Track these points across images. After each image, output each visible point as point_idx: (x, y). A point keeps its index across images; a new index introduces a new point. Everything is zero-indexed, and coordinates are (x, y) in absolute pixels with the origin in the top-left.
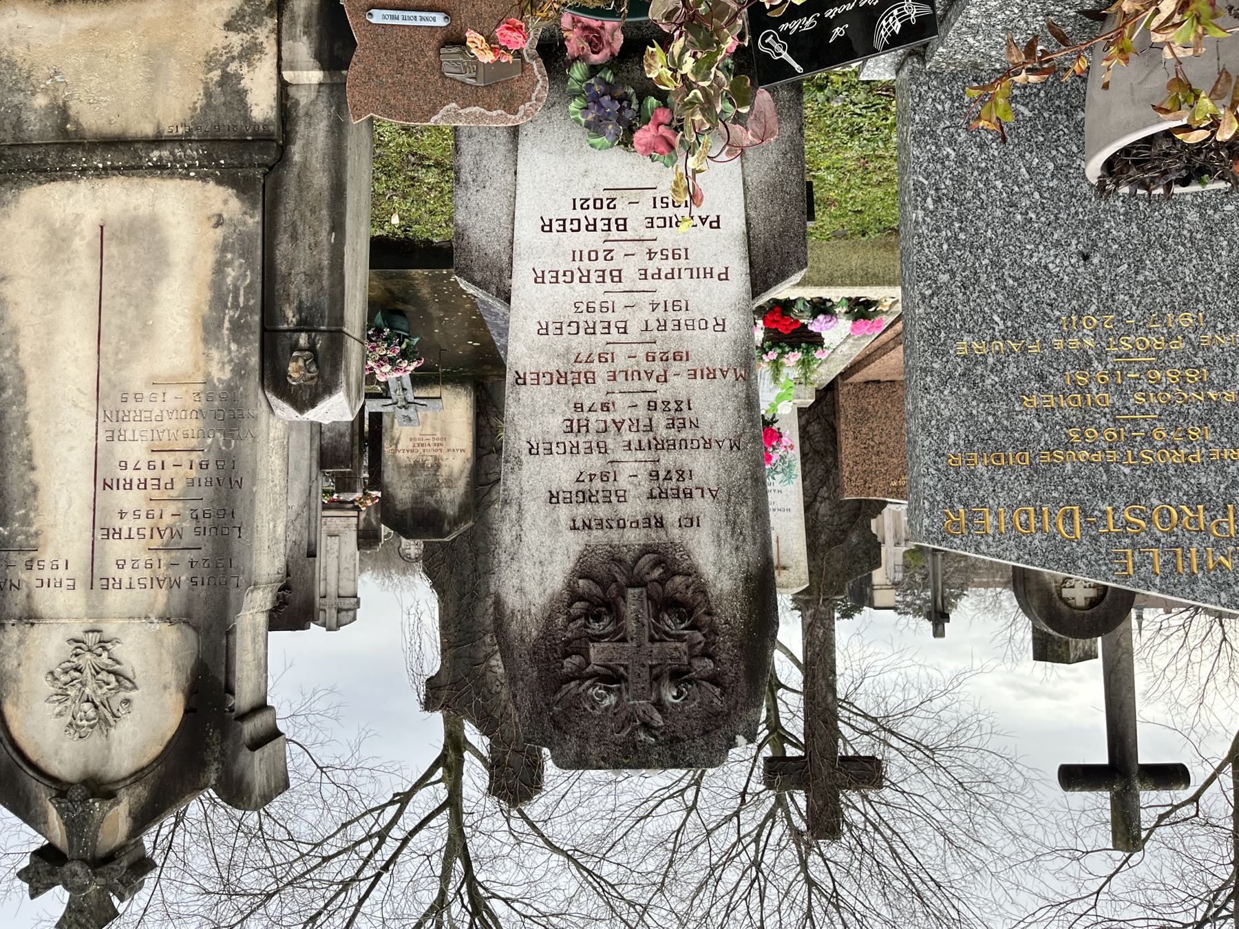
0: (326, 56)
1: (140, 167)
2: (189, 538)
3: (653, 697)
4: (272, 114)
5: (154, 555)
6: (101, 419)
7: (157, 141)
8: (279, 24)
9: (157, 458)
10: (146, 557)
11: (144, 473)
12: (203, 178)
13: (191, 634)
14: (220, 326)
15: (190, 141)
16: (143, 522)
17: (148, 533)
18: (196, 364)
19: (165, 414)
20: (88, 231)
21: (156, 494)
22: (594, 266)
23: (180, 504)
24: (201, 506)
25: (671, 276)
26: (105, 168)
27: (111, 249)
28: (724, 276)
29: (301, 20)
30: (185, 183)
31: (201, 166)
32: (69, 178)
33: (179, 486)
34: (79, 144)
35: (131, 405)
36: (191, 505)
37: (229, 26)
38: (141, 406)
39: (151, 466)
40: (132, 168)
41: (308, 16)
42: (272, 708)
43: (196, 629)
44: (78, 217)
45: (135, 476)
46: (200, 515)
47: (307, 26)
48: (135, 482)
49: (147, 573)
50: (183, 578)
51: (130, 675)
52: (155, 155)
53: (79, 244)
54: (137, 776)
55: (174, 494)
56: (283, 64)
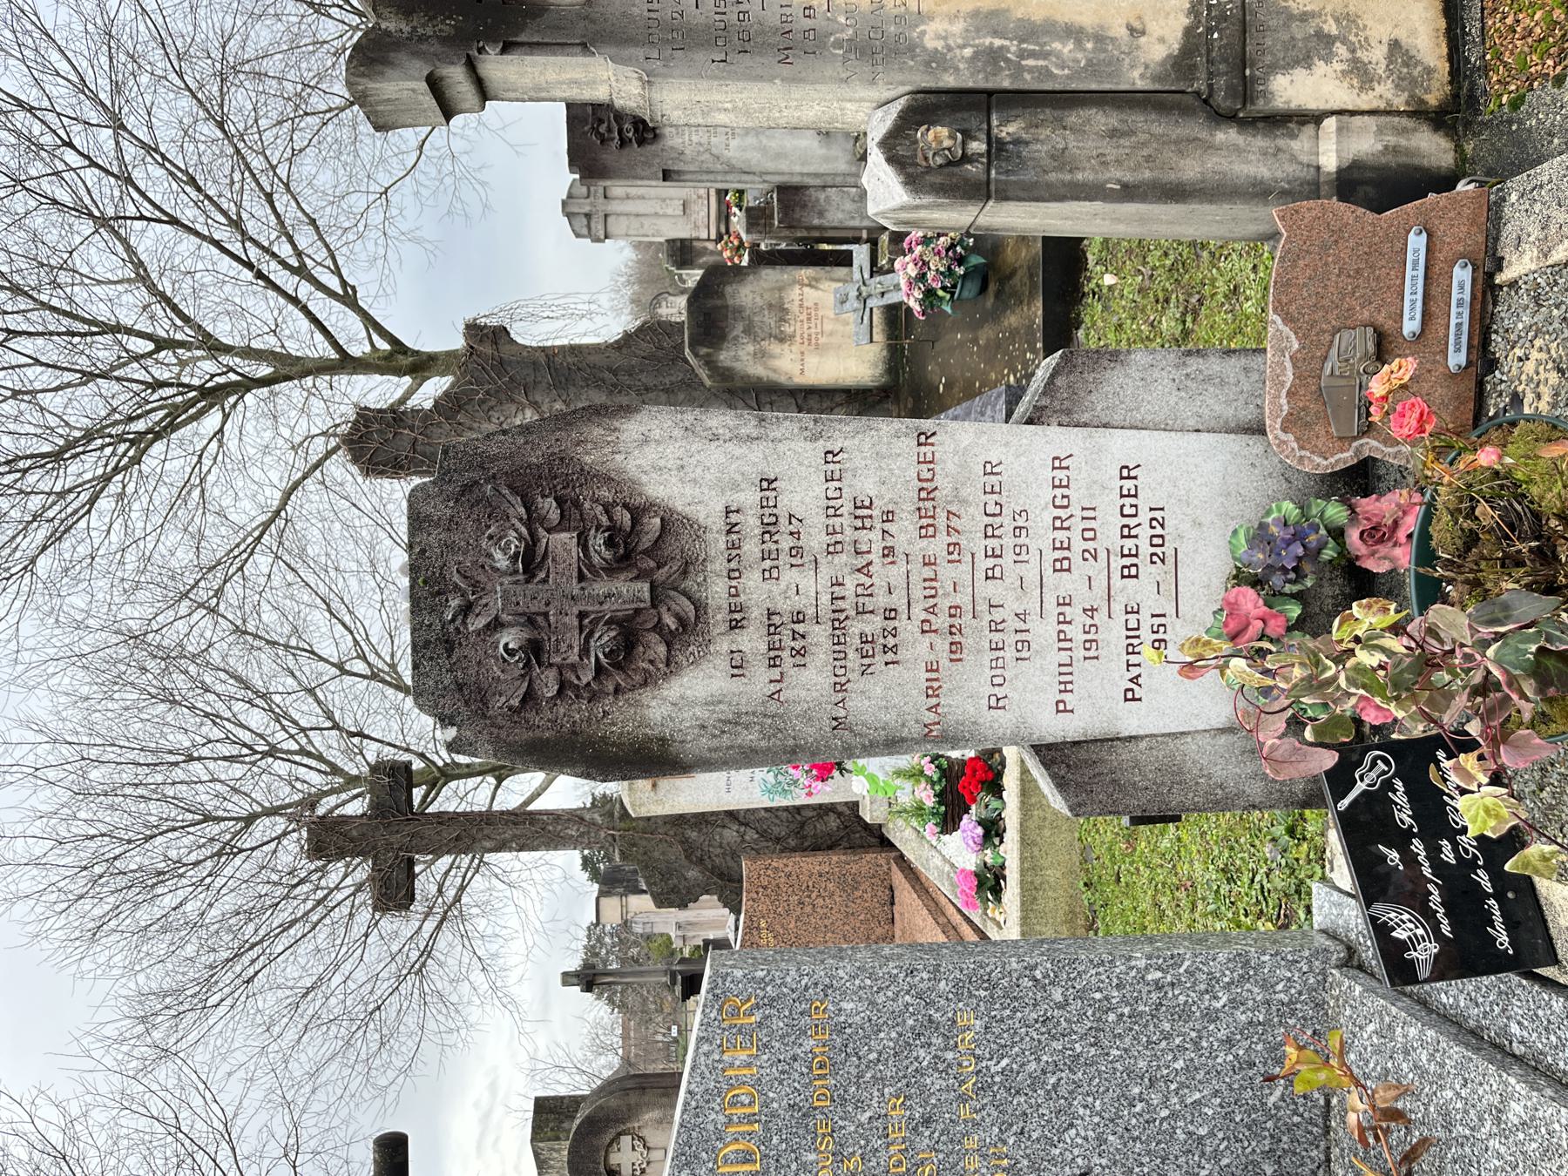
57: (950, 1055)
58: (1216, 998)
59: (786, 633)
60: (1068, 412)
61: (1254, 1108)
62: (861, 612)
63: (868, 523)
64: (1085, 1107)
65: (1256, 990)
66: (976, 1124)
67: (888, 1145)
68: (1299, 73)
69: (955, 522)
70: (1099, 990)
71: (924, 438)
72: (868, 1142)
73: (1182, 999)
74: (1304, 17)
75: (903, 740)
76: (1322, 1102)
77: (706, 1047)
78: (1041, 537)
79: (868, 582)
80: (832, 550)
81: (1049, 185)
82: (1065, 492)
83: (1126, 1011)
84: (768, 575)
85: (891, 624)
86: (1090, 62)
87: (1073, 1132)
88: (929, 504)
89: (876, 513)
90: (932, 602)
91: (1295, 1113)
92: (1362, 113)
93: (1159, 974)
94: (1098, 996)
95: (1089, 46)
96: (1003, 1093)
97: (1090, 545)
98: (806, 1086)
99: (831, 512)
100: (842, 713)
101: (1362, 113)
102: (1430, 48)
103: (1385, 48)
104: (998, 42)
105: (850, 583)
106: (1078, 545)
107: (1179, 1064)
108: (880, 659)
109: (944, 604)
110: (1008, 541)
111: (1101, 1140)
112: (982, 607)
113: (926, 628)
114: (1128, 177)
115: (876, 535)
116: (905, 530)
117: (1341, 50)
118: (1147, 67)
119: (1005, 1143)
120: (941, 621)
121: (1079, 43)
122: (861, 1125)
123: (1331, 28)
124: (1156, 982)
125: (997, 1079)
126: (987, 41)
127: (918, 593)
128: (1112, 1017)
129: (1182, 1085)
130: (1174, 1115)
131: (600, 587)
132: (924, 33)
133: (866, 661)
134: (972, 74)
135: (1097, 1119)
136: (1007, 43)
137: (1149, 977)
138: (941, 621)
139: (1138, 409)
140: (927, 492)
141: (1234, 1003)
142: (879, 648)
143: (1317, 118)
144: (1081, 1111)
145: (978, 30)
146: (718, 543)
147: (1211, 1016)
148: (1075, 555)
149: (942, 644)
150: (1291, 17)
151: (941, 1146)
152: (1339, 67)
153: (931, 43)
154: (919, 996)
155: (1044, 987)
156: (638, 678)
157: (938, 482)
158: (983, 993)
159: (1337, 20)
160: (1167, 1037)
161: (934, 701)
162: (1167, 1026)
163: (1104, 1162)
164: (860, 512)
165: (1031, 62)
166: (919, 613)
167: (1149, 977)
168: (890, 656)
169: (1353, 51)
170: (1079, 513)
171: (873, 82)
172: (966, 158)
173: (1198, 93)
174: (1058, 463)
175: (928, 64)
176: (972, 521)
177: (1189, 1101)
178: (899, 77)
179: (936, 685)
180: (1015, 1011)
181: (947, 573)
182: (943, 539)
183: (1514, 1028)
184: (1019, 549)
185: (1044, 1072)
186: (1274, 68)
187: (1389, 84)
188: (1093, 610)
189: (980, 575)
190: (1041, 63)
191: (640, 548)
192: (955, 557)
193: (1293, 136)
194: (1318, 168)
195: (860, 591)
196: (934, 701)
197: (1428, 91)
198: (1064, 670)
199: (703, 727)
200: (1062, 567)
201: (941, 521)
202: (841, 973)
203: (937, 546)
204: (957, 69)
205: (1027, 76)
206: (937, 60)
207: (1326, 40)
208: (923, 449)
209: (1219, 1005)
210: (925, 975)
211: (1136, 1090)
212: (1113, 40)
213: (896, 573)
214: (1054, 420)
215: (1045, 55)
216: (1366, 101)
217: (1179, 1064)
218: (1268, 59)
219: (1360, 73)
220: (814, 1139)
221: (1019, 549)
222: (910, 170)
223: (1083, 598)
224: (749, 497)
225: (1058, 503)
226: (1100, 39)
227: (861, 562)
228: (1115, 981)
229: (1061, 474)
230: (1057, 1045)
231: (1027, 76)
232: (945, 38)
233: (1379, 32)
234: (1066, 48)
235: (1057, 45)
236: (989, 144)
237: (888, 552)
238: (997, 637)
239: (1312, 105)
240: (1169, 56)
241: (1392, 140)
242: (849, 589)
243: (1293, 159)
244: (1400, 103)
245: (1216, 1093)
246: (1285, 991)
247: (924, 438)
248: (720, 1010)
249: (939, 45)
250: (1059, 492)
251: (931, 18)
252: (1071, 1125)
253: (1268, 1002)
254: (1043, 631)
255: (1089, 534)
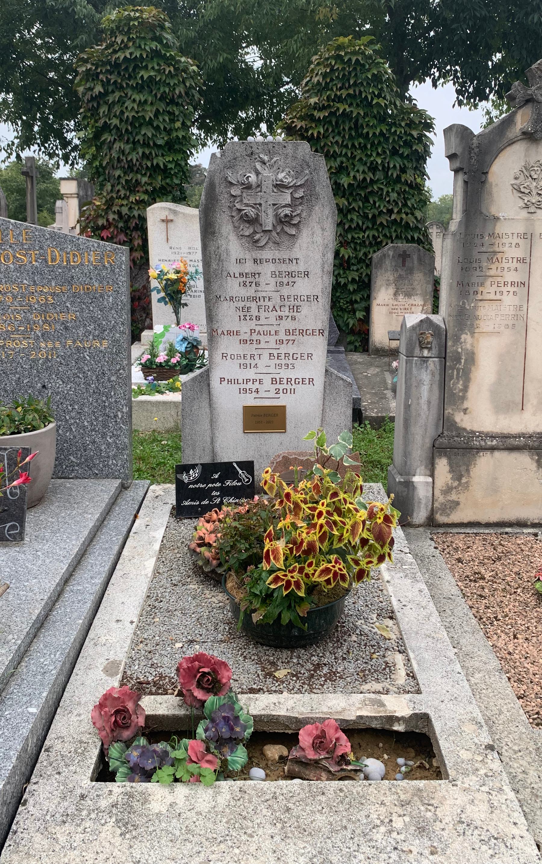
0: (411, 488)
1: (503, 437)
2: (484, 257)
3: (260, 176)
4: (437, 461)
5: (501, 249)
6: (525, 316)
7: (493, 449)
8: (433, 504)
9: (498, 297)
10: (505, 249)
11: (505, 289)
12: (473, 432)
13: (484, 211)
14: (466, 360)
15: (477, 449)
16: (506, 266)
17: (504, 260)
18: (478, 341)
19: (494, 318)
20: (529, 407)
21: (499, 279)
22: (285, 386)
23: (488, 274)
24: (478, 273)
25: (248, 380)
26: (520, 437)
27: (519, 399)
28: (222, 380)
29: (422, 506)
30: (482, 429)
31: (473, 437)
32: (538, 433)
33: (488, 283)
34: (532, 449)
35: (510, 323)
36: (483, 274)
37: (458, 503)
38: (506, 322)
39: (502, 293)
40: (506, 437)
41: (419, 507)
42: (452, 170)
43: (481, 213)
44: (534, 414)
45: (509, 288)
46: (478, 269)
47: (420, 502)
48: (509, 285)
49: (504, 241)
50: (487, 238)
51: (515, 191)
52: (495, 442)
53: (535, 402)
54: (511, 143)
55: (491, 279)
56: (431, 485)
57: (91, 337)
58: (111, 438)
59: (252, 279)
60: (330, 385)
61: (69, 451)
62: (259, 307)
63: (291, 311)
64: (70, 388)
65: (113, 453)
66: (65, 346)
67: (57, 313)
68: (447, 468)
69: (291, 342)
70: (115, 394)
71: (321, 332)
72: (59, 305)
73: (111, 425)
74: (468, 471)
75: (212, 321)
76: (71, 476)
77: (96, 245)
78: (285, 374)
79: (270, 310)
80: (282, 297)
81: (411, 379)
82: (301, 383)
83: (107, 404)
84: (273, 274)
85: (254, 319)
86: (455, 394)
87: (61, 383)
88: (297, 333)
89: (295, 314)
90: (262, 333)
91: (67, 466)
92: (433, 491)
93: (120, 417)
94: (112, 393)
95: (461, 394)
96: (76, 357)
97: (281, 391)
98: (80, 283)
99: (296, 297)
100: (222, 299)
101: (433, 491)
102: (456, 517)
103: (456, 500)
104: (463, 361)
105: (270, 304)
106: (281, 387)
107: (86, 423)
108: (242, 314)
109: (261, 338)
110: (283, 362)
111: (58, 393)
112: (260, 351)
113: (253, 331)
114: (413, 407)
115: (287, 313)
116: (288, 324)
117: (456, 484)
118: (452, 415)
119: (57, 357)
120: (255, 337)
121: (461, 390)
122: (65, 303)
123: (464, 480)
124: (117, 416)
125: (82, 355)
126: (463, 357)
127: (265, 328)
128: (104, 399)
129: (78, 424)
130: (67, 421)
131: (270, 212)
132: (467, 334)
133: (241, 309)
134: (451, 351)
135: (66, 392)
136: (463, 364)
137: (119, 413)
138: (255, 337)
139: (330, 411)
140: (302, 332)
141: (109, 444)
142: (245, 313)
143: (432, 475)
144: (69, 386)
145: (467, 354)
146: (285, 255)
147: (104, 436)
148: (278, 386)
149: (247, 337)
150: (468, 466)
151: (56, 333)
152: (450, 483)
153: (463, 337)
154: (114, 326)
155: (116, 373)
156: (237, 224)
157: (306, 337)
158: (114, 350)
159: (467, 483)
160: (96, 419)
161: (226, 333)
162: (100, 419)
163: (50, 394)
164: (295, 307)
165: (455, 373)
166: (258, 328)
167: (119, 413)
168: (242, 318)
169: (455, 488)
170: (293, 387)
171: (450, 315)
172: (422, 348)
173: (442, 433)
174: (311, 380)
175: (456, 335)
176: (291, 349)
177: (72, 427)
178: (451, 325)
179: (232, 334)
180: (107, 362)
181: (272, 339)
182: (285, 338)
183: (112, 522)
184: (280, 365)
185: (84, 373)
186: (449, 459)
187: (443, 501)
188: (258, 392)
189: (271, 351)
190: (455, 376)
191: (285, 228)
192: (278, 342)
193: (426, 467)
194: (414, 475)
195: (267, 307)
196: (226, 333)
197: (441, 514)
198: (236, 381)
199: (218, 248)
200: (274, 381)
201: (291, 337)
202: (123, 297)
203: (282, 336)
204: (454, 346)
205: (450, 371)
206: (457, 339)
207: (459, 478)
208: (318, 331)
209: (108, 439)
210: (122, 329)
211: (76, 407)
212: (463, 403)
213: (273, 320)
214: (327, 380)
215: (458, 378)
216: (437, 493)
217: (86, 423)
218: (453, 457)
219: (448, 490)
220: (60, 285)
221: (280, 365)
222: (418, 329)
223: (262, 388)
224: (302, 268)
225: (297, 380)
226: (463, 398)
227: (277, 308)
228: (118, 400)
229: (307, 381)
230: (94, 378)
231: (450, 371)
232: (465, 342)
233: (463, 498)
234: (460, 386)
235: (461, 382)
236: (427, 357)
237: (281, 318)
238: (249, 357)
239: (436, 473)
240: (456, 423)
241: (423, 501)
242: (267, 303)
243: (418, 467)
244: (436, 505)
245: (75, 437)
246: (113, 464)
247: (321, 332)
248: (110, 251)
249: (462, 340)
250: (301, 380)
251: (472, 337)
252: (63, 382)
253: (108, 457)
254: (250, 374)
255: (285, 391)
